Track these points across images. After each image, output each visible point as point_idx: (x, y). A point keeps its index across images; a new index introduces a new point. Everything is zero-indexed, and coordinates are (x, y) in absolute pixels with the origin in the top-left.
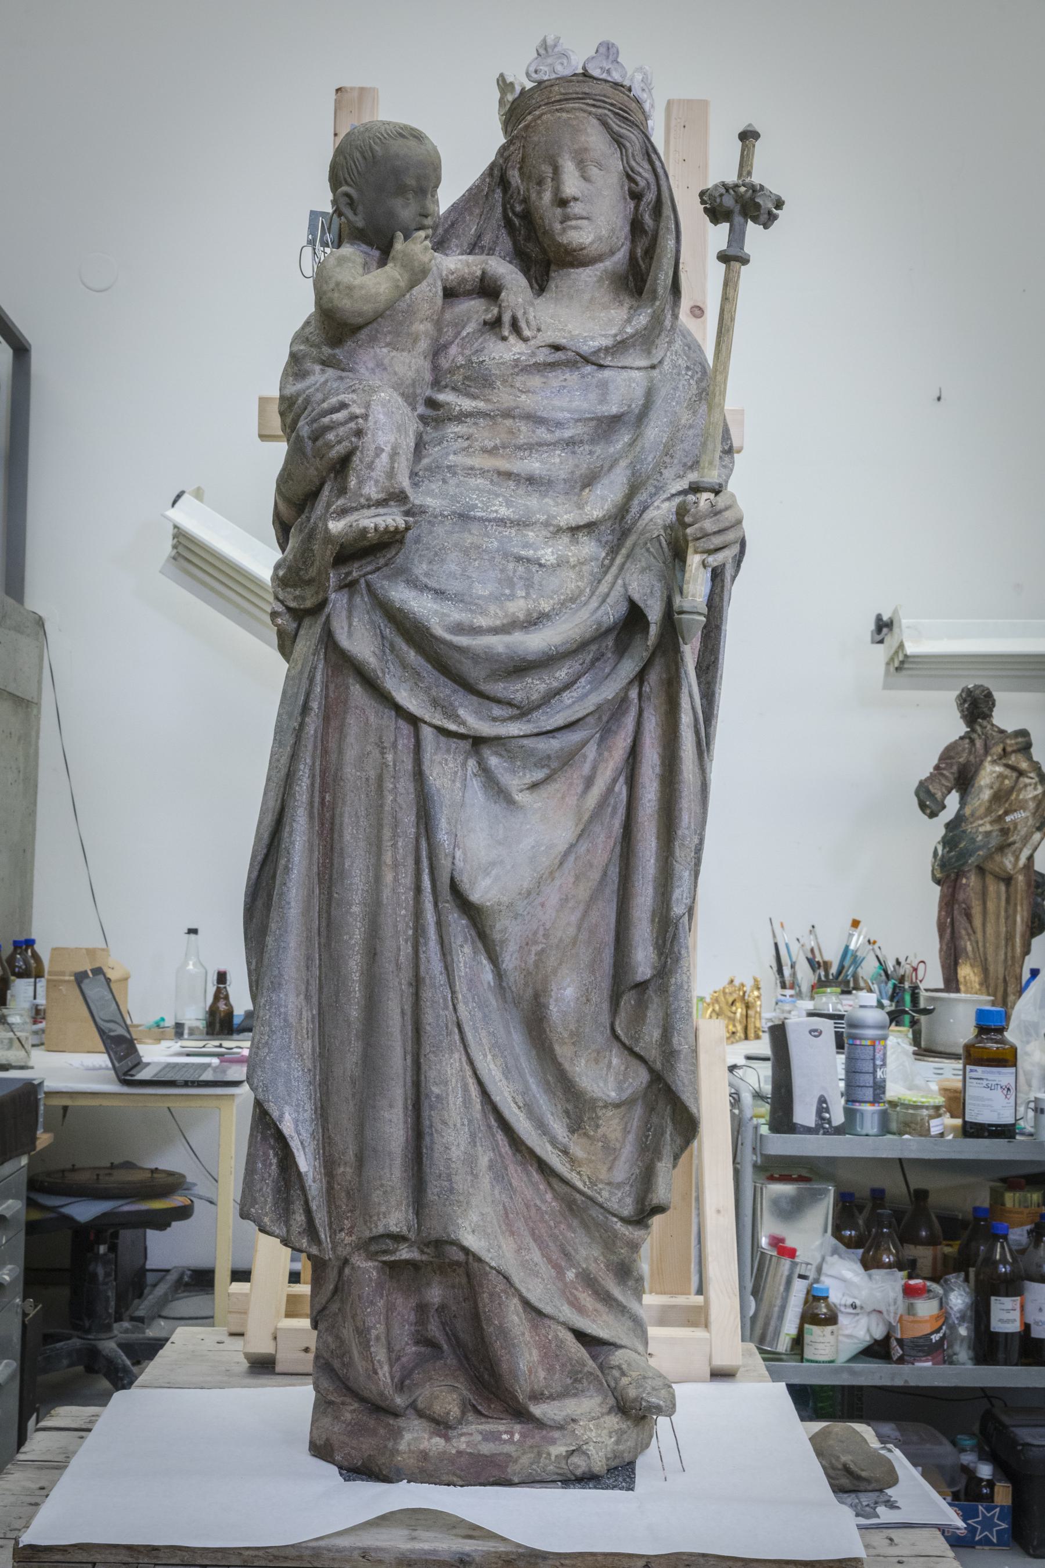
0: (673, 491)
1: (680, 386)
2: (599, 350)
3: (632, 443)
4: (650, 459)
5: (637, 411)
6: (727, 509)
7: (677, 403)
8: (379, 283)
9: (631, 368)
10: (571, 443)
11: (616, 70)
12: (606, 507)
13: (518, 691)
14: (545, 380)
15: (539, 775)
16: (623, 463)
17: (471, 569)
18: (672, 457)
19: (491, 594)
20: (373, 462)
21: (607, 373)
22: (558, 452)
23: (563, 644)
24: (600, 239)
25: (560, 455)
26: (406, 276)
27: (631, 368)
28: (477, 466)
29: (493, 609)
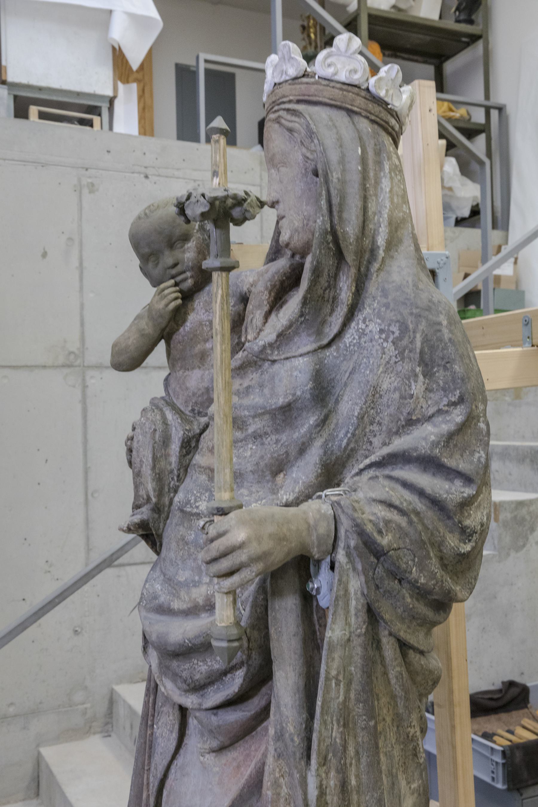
0: (362, 466)
1: (374, 352)
2: (264, 347)
3: (324, 422)
4: (341, 435)
5: (308, 396)
6: (220, 535)
7: (371, 371)
8: (129, 338)
9: (294, 357)
10: (257, 436)
11: (292, 65)
12: (297, 490)
13: (185, 669)
14: (241, 382)
15: (215, 744)
16: (318, 443)
17: (179, 558)
18: (380, 424)
19: (186, 580)
20: (140, 471)
21: (277, 366)
22: (250, 446)
23: (196, 637)
24: (296, 230)
25: (251, 449)
26: (150, 324)
27: (294, 357)
28: (203, 465)
29: (183, 593)
